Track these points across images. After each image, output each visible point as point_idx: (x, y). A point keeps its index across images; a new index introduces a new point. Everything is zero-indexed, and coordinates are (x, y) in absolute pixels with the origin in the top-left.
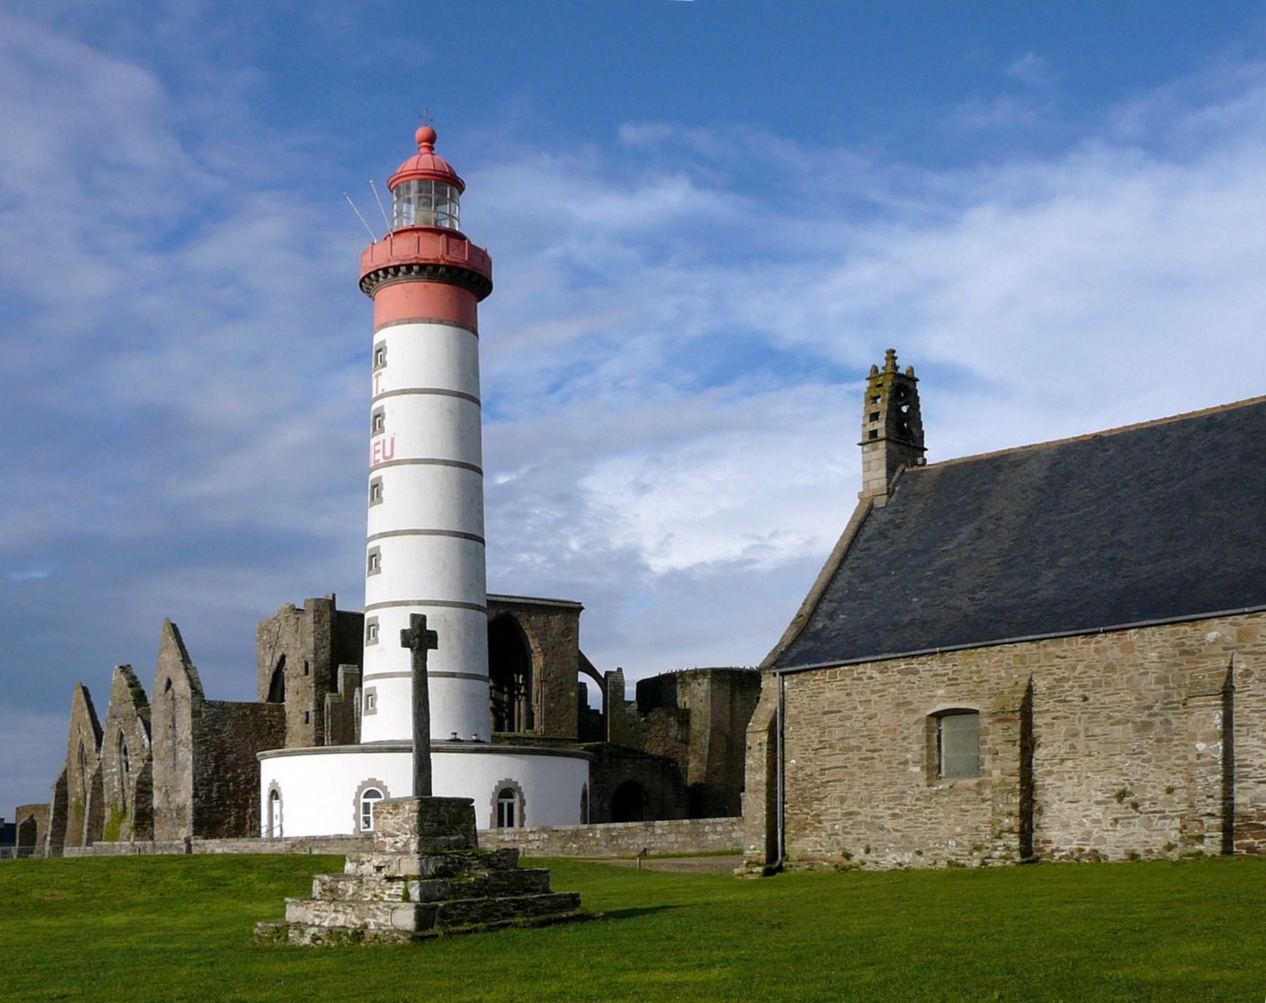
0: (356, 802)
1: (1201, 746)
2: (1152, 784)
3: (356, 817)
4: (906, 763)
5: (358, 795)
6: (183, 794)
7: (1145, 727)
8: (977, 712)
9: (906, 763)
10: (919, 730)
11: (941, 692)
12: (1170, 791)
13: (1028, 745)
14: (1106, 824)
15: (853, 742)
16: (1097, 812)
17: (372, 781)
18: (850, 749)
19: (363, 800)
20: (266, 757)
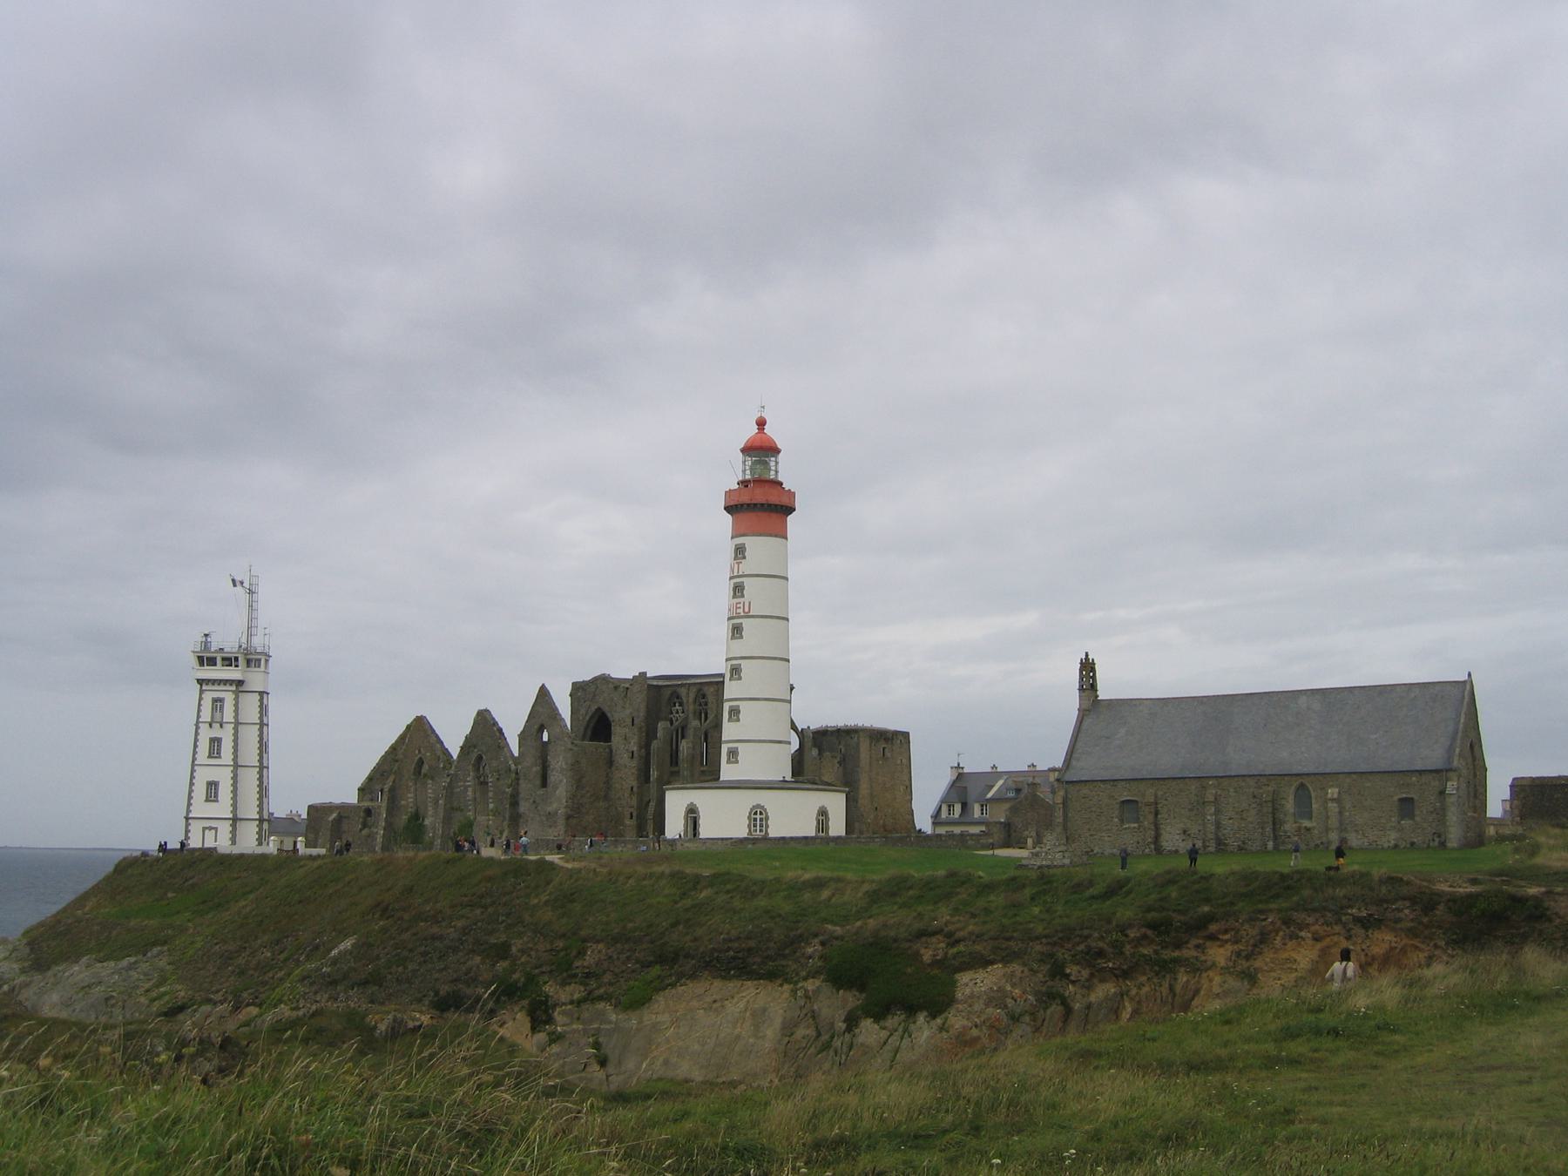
0: (749, 818)
1: (1209, 818)
2: (1194, 830)
3: (749, 826)
4: (1112, 817)
5: (750, 814)
6: (555, 805)
7: (1191, 810)
8: (1136, 802)
9: (1112, 817)
10: (1118, 806)
11: (1125, 794)
12: (1199, 831)
13: (1157, 814)
14: (1180, 841)
15: (1094, 809)
16: (1177, 837)
17: (758, 806)
18: (1092, 811)
19: (753, 816)
20: (668, 789)
